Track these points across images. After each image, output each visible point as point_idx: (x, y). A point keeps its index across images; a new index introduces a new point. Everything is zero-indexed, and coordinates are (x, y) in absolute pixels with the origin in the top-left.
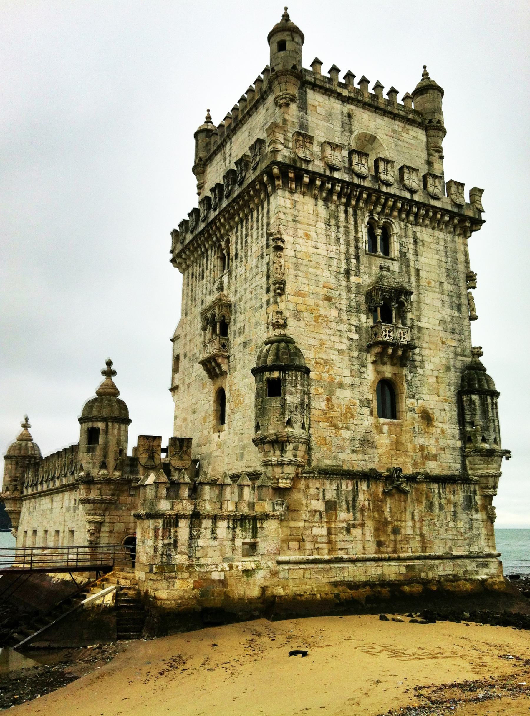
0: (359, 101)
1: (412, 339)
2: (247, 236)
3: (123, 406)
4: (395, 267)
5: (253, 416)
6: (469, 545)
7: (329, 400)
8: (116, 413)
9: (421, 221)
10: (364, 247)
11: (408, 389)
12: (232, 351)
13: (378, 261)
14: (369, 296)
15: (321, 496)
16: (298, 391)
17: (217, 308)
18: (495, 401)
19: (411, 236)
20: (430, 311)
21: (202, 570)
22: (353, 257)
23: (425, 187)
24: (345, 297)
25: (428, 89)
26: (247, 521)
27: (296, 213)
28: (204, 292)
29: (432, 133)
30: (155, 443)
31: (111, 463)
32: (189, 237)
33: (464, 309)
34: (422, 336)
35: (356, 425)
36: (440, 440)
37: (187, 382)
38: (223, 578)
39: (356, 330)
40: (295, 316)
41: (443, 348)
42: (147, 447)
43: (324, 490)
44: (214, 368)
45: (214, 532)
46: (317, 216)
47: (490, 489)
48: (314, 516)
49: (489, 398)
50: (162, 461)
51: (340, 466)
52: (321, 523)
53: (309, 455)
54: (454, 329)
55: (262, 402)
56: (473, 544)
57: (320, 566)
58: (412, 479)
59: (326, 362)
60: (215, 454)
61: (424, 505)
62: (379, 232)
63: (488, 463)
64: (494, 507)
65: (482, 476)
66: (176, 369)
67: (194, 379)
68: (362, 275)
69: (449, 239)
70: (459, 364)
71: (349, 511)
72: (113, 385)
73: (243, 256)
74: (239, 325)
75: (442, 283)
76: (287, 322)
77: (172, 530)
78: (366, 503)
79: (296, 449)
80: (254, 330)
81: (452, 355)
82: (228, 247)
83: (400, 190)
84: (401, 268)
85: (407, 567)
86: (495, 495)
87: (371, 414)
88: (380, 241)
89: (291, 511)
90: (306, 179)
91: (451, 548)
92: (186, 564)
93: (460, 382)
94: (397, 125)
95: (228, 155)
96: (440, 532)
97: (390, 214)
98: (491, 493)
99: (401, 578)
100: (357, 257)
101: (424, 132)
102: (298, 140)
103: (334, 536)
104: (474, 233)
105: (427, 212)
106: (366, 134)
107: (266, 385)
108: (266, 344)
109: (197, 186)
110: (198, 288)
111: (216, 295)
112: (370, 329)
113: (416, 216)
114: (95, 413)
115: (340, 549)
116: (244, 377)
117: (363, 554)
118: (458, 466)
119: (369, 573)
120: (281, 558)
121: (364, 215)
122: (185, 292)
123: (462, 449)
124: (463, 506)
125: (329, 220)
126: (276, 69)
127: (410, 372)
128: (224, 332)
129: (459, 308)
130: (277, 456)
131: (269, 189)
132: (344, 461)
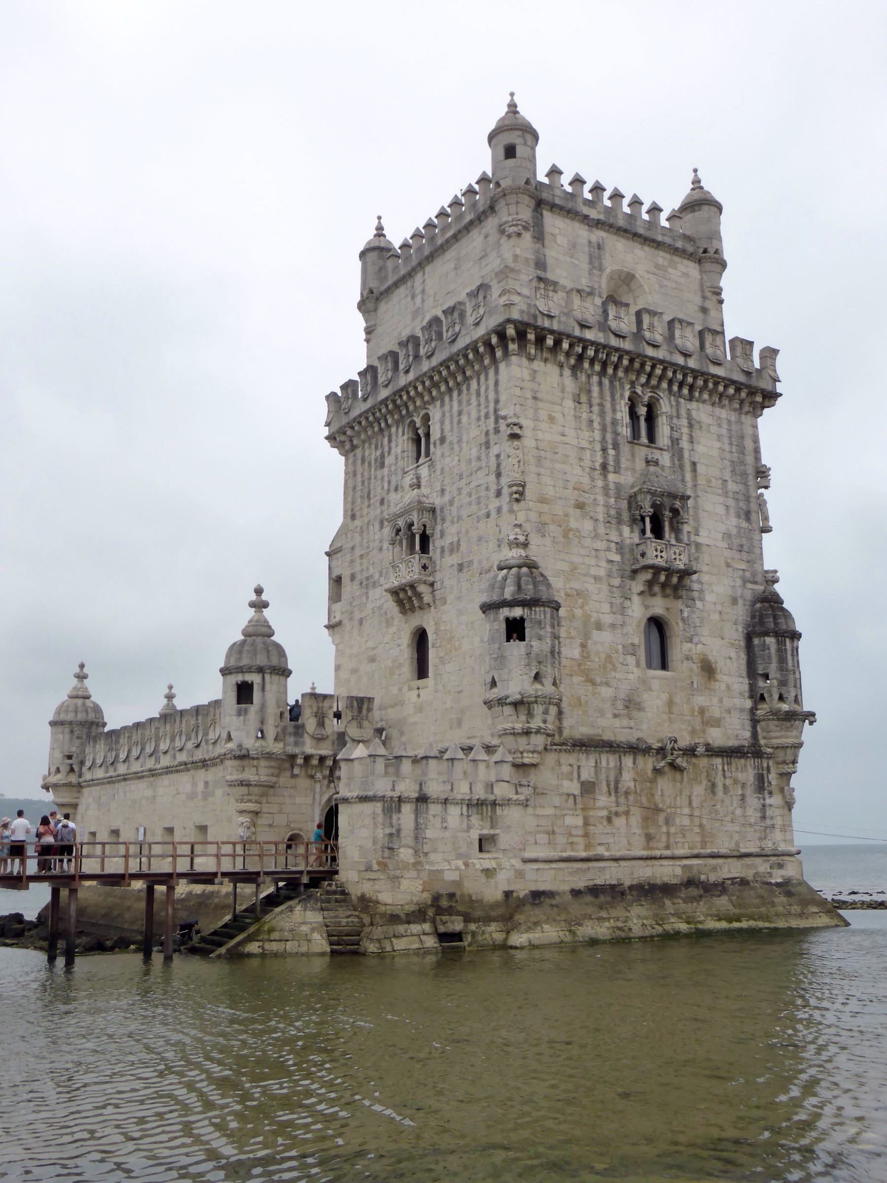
0: (611, 226)
2: (460, 413)
3: (280, 651)
4: (665, 459)
7: (583, 646)
8: (275, 661)
9: (697, 394)
10: (624, 433)
11: (685, 630)
12: (438, 576)
13: (642, 452)
14: (632, 501)
15: (575, 775)
16: (549, 635)
17: (415, 514)
20: (710, 522)
21: (432, 868)
22: (610, 446)
24: (602, 503)
25: (701, 204)
26: (484, 807)
27: (535, 386)
29: (708, 266)
30: (326, 704)
31: (271, 732)
33: (754, 516)
35: (619, 680)
36: (725, 700)
37: (357, 616)
38: (458, 879)
39: (617, 549)
40: (539, 531)
42: (315, 709)
43: (579, 767)
44: (410, 598)
45: (444, 820)
46: (563, 391)
48: (567, 801)
49: (787, 640)
52: (576, 810)
54: (742, 546)
55: (499, 649)
56: (765, 838)
58: (690, 752)
59: (579, 593)
62: (642, 411)
63: (788, 729)
64: (793, 790)
65: (777, 748)
67: (371, 612)
68: (622, 471)
69: (733, 419)
70: (748, 595)
71: (610, 794)
72: (266, 621)
73: (455, 441)
74: (449, 539)
75: (726, 481)
77: (395, 817)
78: (632, 784)
79: (546, 712)
80: (476, 548)
81: (739, 582)
83: (671, 353)
85: (684, 866)
87: (638, 665)
89: (538, 794)
90: (550, 342)
91: (737, 844)
92: (412, 861)
94: (662, 258)
95: (418, 290)
97: (658, 386)
98: (789, 770)
100: (616, 446)
101: (697, 266)
102: (539, 288)
103: (591, 827)
105: (706, 382)
106: (621, 271)
107: (504, 626)
108: (501, 569)
110: (373, 480)
112: (635, 547)
113: (692, 388)
114: (245, 661)
116: (460, 612)
117: (628, 850)
118: (748, 734)
119: (636, 876)
120: (528, 855)
122: (350, 484)
123: (753, 711)
124: (753, 787)
125: (579, 395)
126: (503, 184)
127: (687, 606)
128: (425, 549)
129: (747, 515)
130: (521, 722)
131: (499, 353)
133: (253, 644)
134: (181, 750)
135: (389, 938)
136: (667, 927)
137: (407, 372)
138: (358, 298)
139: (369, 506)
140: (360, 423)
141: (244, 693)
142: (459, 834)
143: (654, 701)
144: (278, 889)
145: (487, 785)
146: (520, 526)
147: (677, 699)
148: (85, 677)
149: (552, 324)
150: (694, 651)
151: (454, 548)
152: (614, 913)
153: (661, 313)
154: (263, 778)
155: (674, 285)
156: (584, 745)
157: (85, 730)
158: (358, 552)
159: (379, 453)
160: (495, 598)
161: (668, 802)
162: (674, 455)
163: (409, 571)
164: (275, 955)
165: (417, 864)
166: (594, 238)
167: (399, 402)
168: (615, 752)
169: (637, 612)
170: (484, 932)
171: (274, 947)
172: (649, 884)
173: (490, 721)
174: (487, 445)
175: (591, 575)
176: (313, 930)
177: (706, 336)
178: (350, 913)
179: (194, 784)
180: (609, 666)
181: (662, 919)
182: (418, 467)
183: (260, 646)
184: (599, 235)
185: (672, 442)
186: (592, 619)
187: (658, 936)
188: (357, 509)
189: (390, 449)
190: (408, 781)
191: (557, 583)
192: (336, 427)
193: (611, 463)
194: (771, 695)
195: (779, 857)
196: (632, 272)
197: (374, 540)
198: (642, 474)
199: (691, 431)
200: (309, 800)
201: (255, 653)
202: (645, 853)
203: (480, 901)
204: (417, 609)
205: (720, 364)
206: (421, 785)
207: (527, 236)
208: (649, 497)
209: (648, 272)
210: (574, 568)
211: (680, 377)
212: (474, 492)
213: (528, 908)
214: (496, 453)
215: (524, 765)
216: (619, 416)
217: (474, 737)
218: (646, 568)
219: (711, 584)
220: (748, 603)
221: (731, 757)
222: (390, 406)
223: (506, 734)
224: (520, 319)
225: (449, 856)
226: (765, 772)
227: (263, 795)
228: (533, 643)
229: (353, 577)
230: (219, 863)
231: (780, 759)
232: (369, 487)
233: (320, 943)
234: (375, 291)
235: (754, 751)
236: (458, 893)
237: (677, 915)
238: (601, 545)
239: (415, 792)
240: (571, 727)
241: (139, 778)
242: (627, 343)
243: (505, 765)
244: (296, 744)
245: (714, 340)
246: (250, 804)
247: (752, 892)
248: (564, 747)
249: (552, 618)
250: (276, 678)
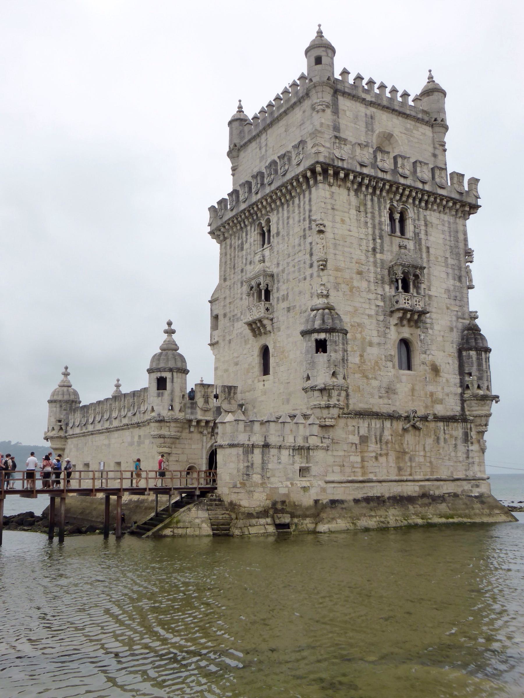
0: (379, 105)
2: (288, 218)
4: (411, 245)
6: (466, 470)
7: (361, 356)
8: (179, 365)
9: (430, 206)
11: (422, 347)
12: (275, 315)
13: (397, 241)
14: (391, 270)
15: (356, 432)
17: (262, 278)
18: (487, 356)
20: (437, 282)
21: (272, 486)
22: (378, 237)
23: (433, 178)
24: (373, 271)
25: (433, 91)
27: (333, 202)
29: (437, 129)
30: (210, 390)
31: (177, 407)
33: (463, 279)
34: (431, 302)
35: (382, 376)
36: (445, 388)
37: (228, 338)
38: (287, 492)
40: (335, 288)
42: (203, 393)
43: (359, 427)
44: (259, 328)
45: (279, 458)
46: (350, 205)
48: (351, 447)
49: (483, 353)
51: (371, 409)
52: (357, 452)
54: (456, 297)
56: (468, 470)
58: (424, 419)
59: (359, 325)
61: (432, 440)
62: (397, 216)
63: (482, 405)
64: (485, 441)
65: (476, 416)
66: (215, 326)
67: (235, 335)
68: (385, 252)
69: (452, 221)
70: (460, 326)
71: (377, 443)
72: (174, 341)
73: (285, 235)
74: (281, 293)
75: (447, 258)
77: (250, 456)
78: (390, 437)
79: (339, 395)
80: (298, 298)
81: (454, 318)
83: (414, 181)
84: (415, 246)
85: (420, 486)
87: (394, 367)
89: (334, 443)
90: (342, 175)
91: (452, 473)
92: (260, 482)
94: (409, 124)
95: (263, 144)
97: (407, 201)
100: (381, 237)
102: (336, 143)
103: (366, 463)
105: (435, 199)
107: (314, 344)
108: (312, 310)
109: (232, 168)
110: (236, 258)
113: (427, 202)
114: (162, 365)
115: (370, 473)
116: (288, 336)
118: (459, 408)
119: (392, 491)
120: (328, 479)
122: (223, 260)
123: (462, 395)
124: (462, 440)
125: (359, 207)
126: (314, 80)
127: (423, 333)
128: (267, 298)
129: (460, 279)
130: (324, 401)
131: (311, 182)
133: (166, 355)
134: (125, 417)
135: (247, 527)
136: (410, 521)
137: (257, 193)
138: (228, 150)
139: (234, 273)
140: (229, 224)
141: (161, 384)
143: (403, 388)
144: (182, 498)
145: (304, 437)
146: (324, 285)
147: (417, 388)
148: (68, 374)
149: (343, 164)
151: (285, 298)
152: (379, 513)
153: (409, 158)
154: (173, 433)
155: (416, 140)
156: (361, 414)
157: (68, 405)
159: (240, 242)
160: (309, 328)
161: (411, 448)
163: (258, 312)
164: (181, 536)
165: (262, 484)
167: (252, 211)
168: (380, 419)
169: (394, 335)
170: (302, 524)
171: (180, 531)
172: (400, 496)
173: (306, 400)
174: (305, 237)
175: (366, 314)
176: (202, 522)
178: (224, 512)
179: (132, 437)
180: (377, 368)
181: (407, 517)
182: (263, 250)
183: (170, 356)
185: (415, 234)
186: (367, 340)
187: (405, 526)
188: (227, 275)
189: (247, 239)
190: (257, 435)
192: (214, 226)
193: (378, 247)
194: (473, 385)
195: (476, 481)
196: (391, 132)
197: (237, 294)
198: (396, 254)
199: (426, 228)
200: (200, 446)
201: (168, 360)
202: (397, 478)
203: (300, 506)
204: (263, 334)
205: (444, 188)
206: (265, 437)
207: (329, 111)
208: (401, 268)
209: (401, 133)
210: (356, 310)
211: (420, 196)
212: (296, 265)
213: (328, 509)
215: (326, 426)
216: (383, 219)
217: (297, 409)
218: (399, 310)
219: (438, 319)
220: (460, 331)
221: (449, 422)
222: (247, 214)
223: (315, 408)
225: (282, 478)
226: (469, 431)
227: (173, 443)
228: (331, 354)
229: (225, 315)
230: (121, 483)
231: (478, 423)
232: (234, 262)
233: (207, 529)
234: (237, 145)
235: (463, 418)
236: (287, 501)
237: (416, 514)
238: (372, 296)
240: (354, 404)
241: (101, 433)
243: (315, 426)
244: (192, 413)
245: (440, 173)
246: (165, 449)
247: (460, 502)
248: (350, 416)
249: (343, 339)
250: (180, 375)
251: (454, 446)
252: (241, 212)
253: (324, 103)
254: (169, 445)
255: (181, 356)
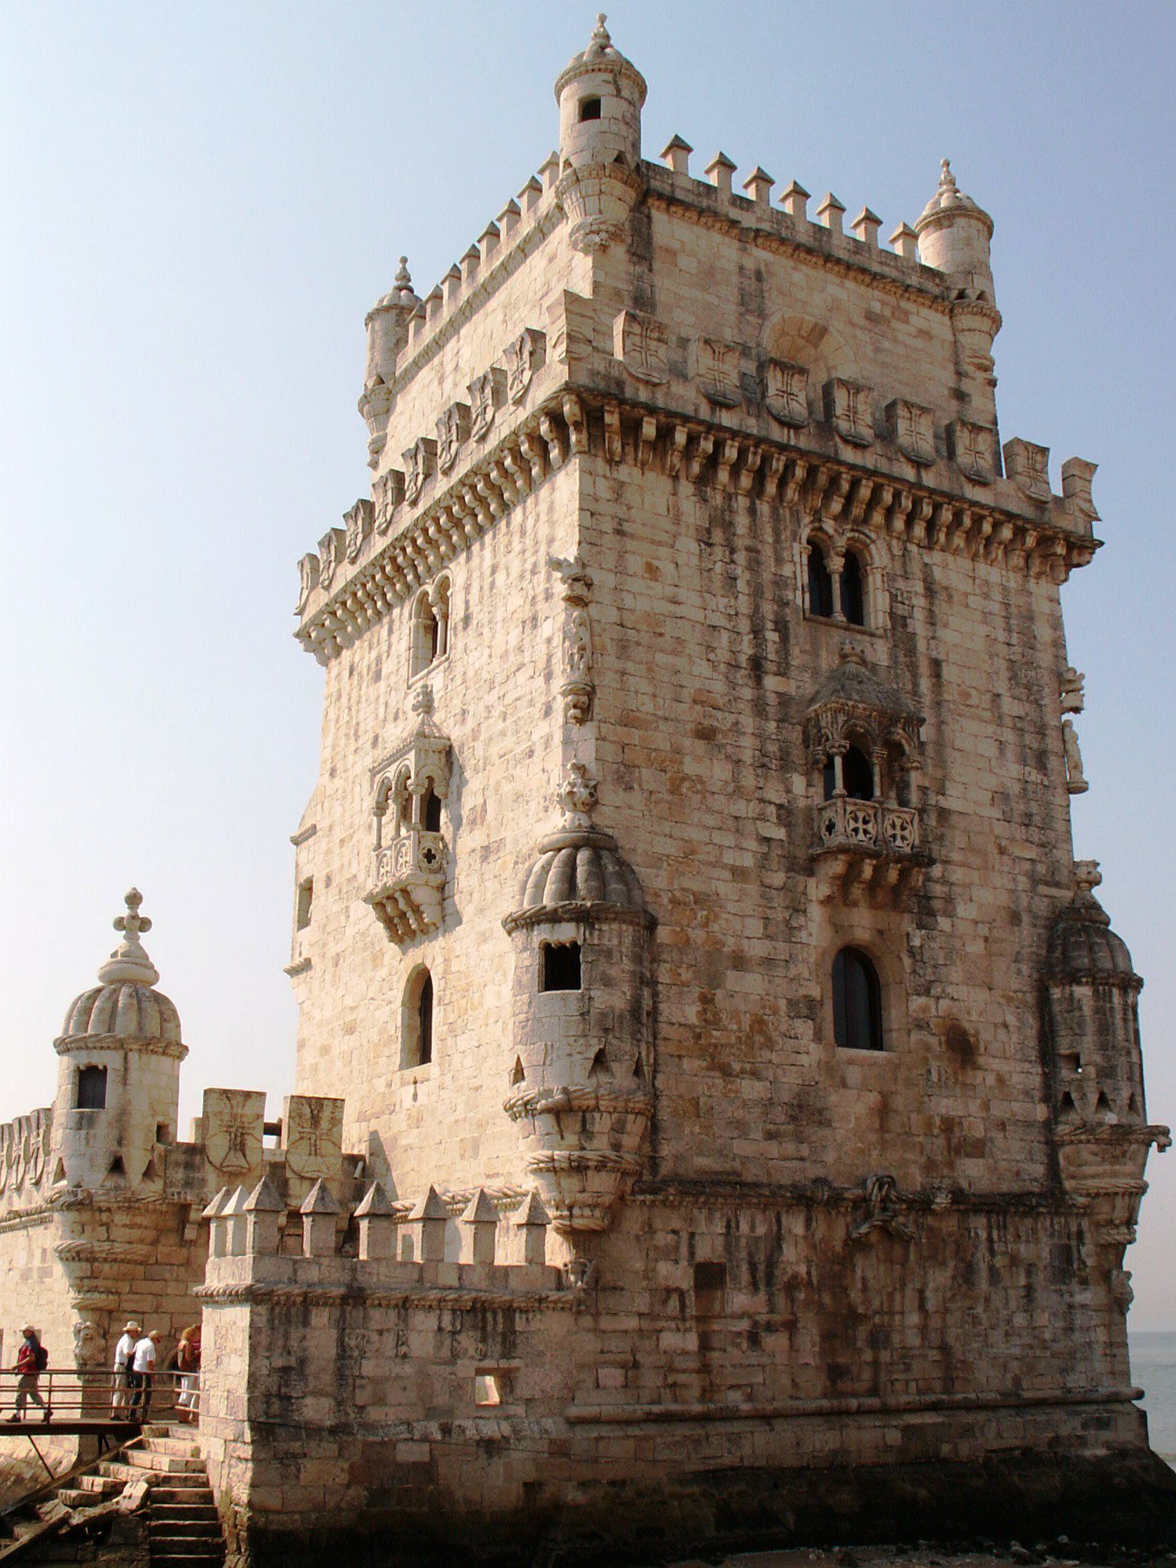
0: (783, 241)
1: (924, 841)
2: (494, 570)
3: (165, 1010)
4: (880, 653)
5: (507, 1042)
6: (1064, 1371)
7: (706, 1000)
9: (942, 537)
10: (799, 601)
11: (914, 972)
13: (836, 636)
15: (684, 1250)
17: (412, 755)
19: (919, 575)
21: (371, 1438)
22: (770, 625)
23: (951, 454)
24: (750, 730)
27: (622, 512)
28: (381, 716)
29: (966, 321)
30: (249, 1110)
31: (136, 1163)
32: (346, 572)
33: (1053, 762)
37: (333, 949)
38: (426, 1458)
39: (778, 817)
40: (619, 779)
41: (1001, 864)
43: (692, 1235)
44: (405, 914)
45: (401, 1341)
46: (677, 520)
47: (1117, 1226)
48: (665, 1302)
49: (1115, 991)
50: (267, 1157)
51: (735, 1173)
52: (684, 1319)
53: (654, 1145)
54: (1029, 815)
57: (681, 1431)
58: (922, 1204)
60: (403, 1142)
61: (949, 1272)
62: (836, 564)
63: (1115, 1159)
64: (1128, 1275)
65: (1097, 1195)
68: (793, 673)
69: (1012, 585)
70: (1042, 907)
73: (485, 621)
75: (999, 695)
76: (599, 794)
77: (295, 1333)
78: (802, 1269)
79: (619, 1128)
80: (511, 815)
81: (1023, 883)
82: (444, 599)
83: (890, 459)
84: (893, 656)
85: (907, 1429)
86: (1130, 1242)
87: (818, 1037)
88: (838, 590)
89: (604, 1289)
90: (649, 429)
91: (1017, 1381)
93: (1044, 952)
95: (449, 367)
96: (991, 1340)
97: (866, 520)
99: (890, 1458)
103: (716, 1354)
104: (1074, 572)
105: (958, 515)
110: (363, 705)
111: (413, 721)
113: (931, 525)
115: (731, 1387)
116: (484, 938)
117: (791, 1397)
118: (1039, 1170)
120: (573, 1411)
121: (799, 521)
122: (332, 716)
123: (1048, 1126)
125: (709, 531)
127: (920, 926)
128: (431, 821)
130: (569, 1148)
131: (554, 453)
132: (745, 1160)
142: (433, 1369)
143: (851, 1108)
147: (899, 1102)
150: (933, 1013)
154: (118, 1248)
158: (339, 833)
159: (374, 654)
160: (526, 906)
161: (876, 1304)
162: (896, 646)
165: (333, 1431)
166: (750, 264)
167: (400, 559)
175: (725, 866)
177: (958, 434)
182: (429, 673)
184: (760, 255)
186: (725, 949)
189: (390, 646)
191: (656, 880)
193: (770, 657)
194: (1083, 1096)
199: (931, 604)
204: (419, 934)
207: (619, 252)
210: (690, 852)
214: (546, 634)
216: (787, 570)
224: (591, 385)
226: (1073, 1243)
228: (593, 993)
229: (328, 881)
239: (340, 1284)
240: (678, 1157)
242: (802, 438)
246: (96, 1295)
248: (661, 1197)
249: (635, 942)
251: (1022, 1292)
252: (373, 564)
253: (603, 227)
254: (109, 1283)
255: (160, 1000)
